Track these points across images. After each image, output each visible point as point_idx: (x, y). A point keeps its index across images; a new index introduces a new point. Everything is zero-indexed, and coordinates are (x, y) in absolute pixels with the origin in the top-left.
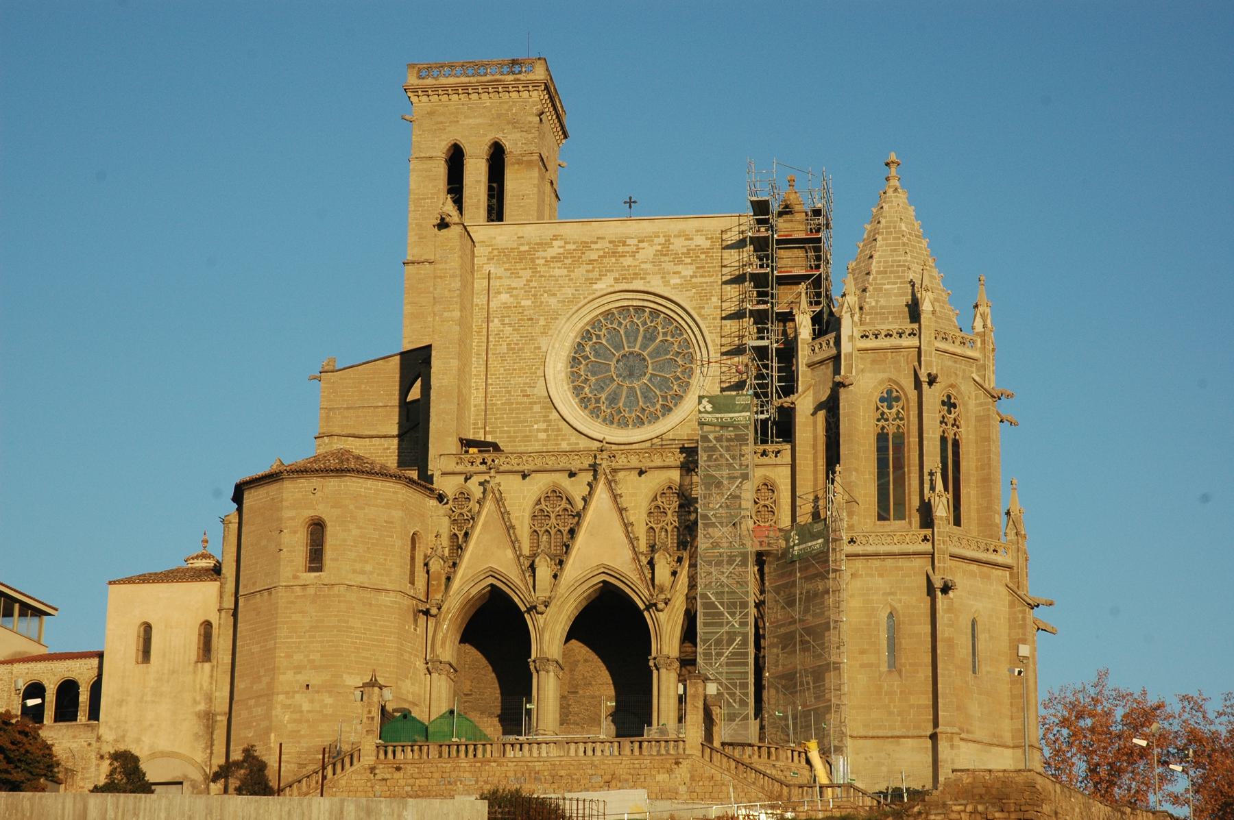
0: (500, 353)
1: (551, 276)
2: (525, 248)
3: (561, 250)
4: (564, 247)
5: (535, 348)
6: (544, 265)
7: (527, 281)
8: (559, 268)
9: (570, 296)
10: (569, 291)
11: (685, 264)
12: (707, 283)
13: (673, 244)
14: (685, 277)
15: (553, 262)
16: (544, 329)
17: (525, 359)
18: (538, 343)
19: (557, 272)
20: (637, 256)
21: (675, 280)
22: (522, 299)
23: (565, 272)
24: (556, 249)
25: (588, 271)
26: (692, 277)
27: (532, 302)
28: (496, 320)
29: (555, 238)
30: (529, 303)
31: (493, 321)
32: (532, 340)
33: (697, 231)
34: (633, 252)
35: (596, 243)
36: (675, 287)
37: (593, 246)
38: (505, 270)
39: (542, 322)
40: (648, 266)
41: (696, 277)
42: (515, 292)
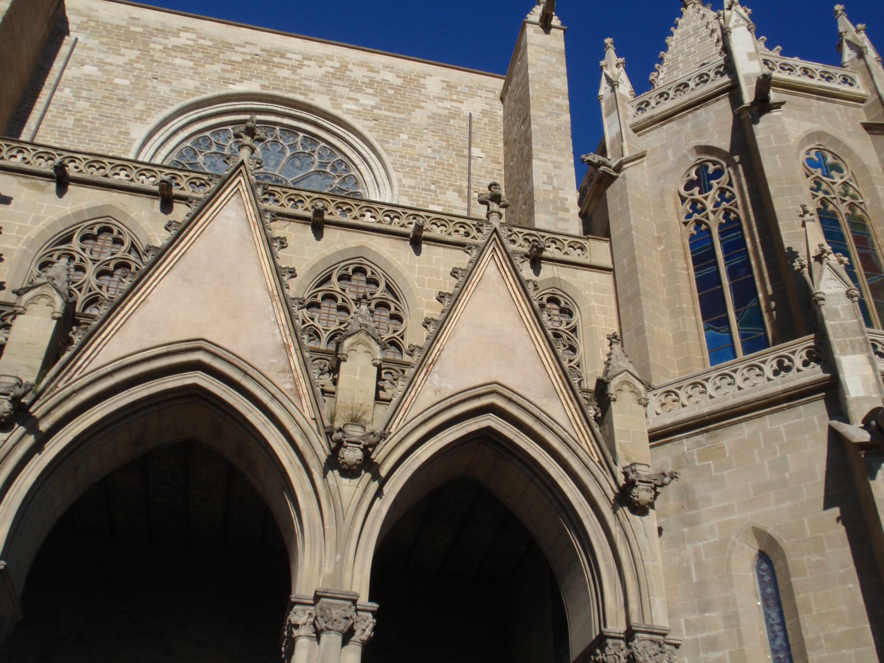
0: (60, 127)
1: (169, 64)
2: (140, 30)
3: (191, 43)
4: (197, 41)
5: (120, 133)
6: (160, 51)
7: (131, 60)
8: (182, 58)
9: (192, 88)
10: (190, 84)
11: (365, 93)
12: (395, 118)
13: (351, 71)
14: (361, 105)
15: (175, 51)
16: (142, 115)
17: (100, 142)
18: (128, 129)
19: (178, 61)
20: (299, 71)
21: (352, 106)
22: (116, 77)
23: (191, 64)
24: (184, 39)
25: (224, 70)
26: (373, 107)
27: (131, 83)
28: (67, 91)
29: (186, 30)
30: (127, 82)
31: (62, 90)
32: (114, 122)
33: (386, 67)
34: (293, 66)
35: (243, 47)
36: (348, 111)
37: (237, 49)
38: (101, 43)
39: (140, 106)
40: (313, 85)
41: (380, 109)
42: (107, 67)
